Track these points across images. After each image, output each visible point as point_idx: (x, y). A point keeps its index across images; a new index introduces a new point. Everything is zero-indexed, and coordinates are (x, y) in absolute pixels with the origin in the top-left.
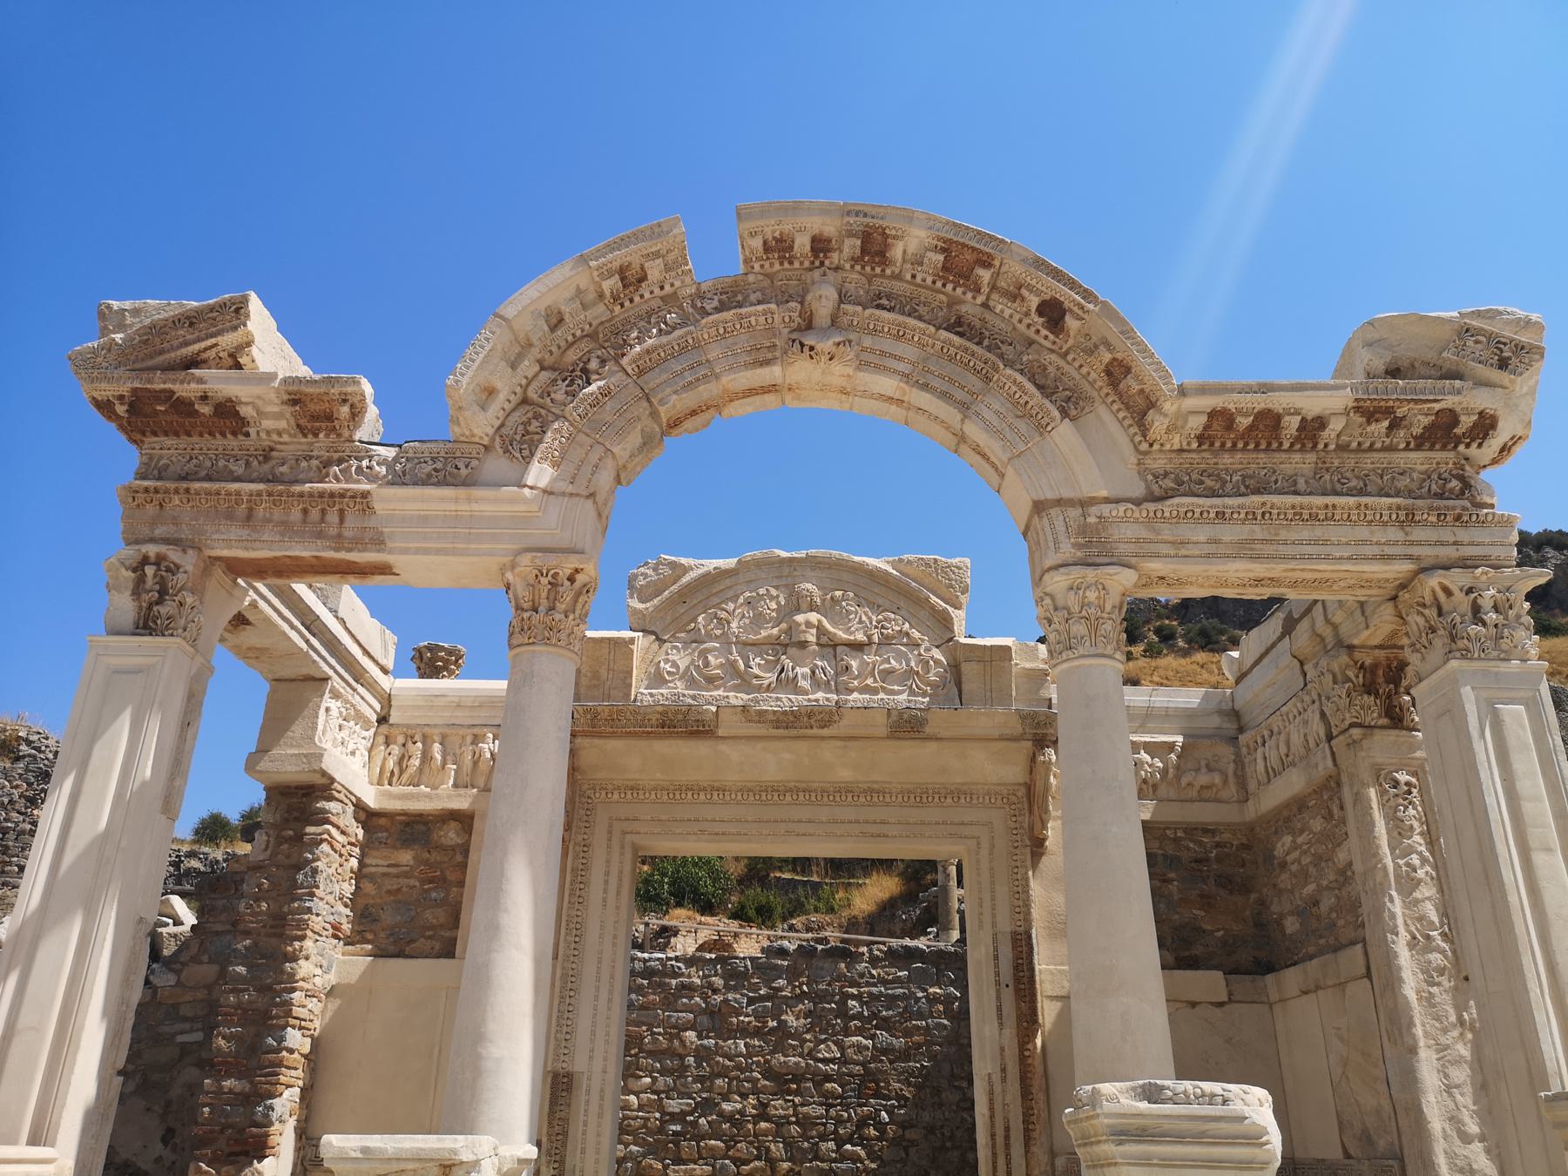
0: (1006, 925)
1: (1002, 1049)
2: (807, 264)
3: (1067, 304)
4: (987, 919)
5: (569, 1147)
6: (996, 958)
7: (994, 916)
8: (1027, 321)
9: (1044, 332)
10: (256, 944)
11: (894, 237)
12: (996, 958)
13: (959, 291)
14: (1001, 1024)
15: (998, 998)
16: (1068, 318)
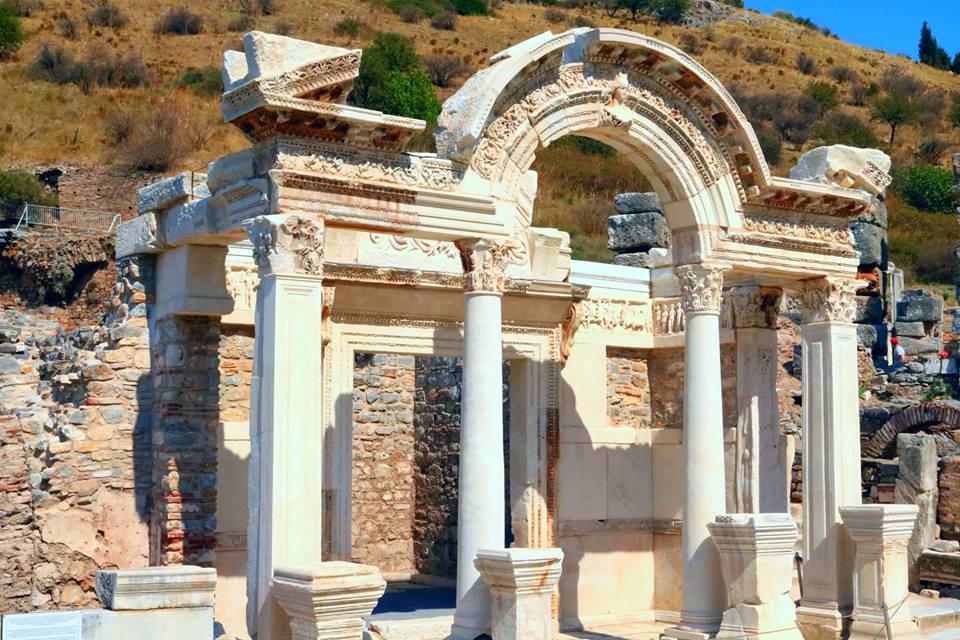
0: (544, 406)
1: (539, 471)
2: (614, 62)
3: (730, 118)
4: (536, 399)
5: (333, 531)
6: (539, 422)
7: (539, 399)
8: (706, 119)
9: (712, 127)
10: (186, 422)
11: (662, 60)
12: (539, 422)
13: (680, 93)
14: (539, 459)
15: (539, 444)
16: (729, 126)
